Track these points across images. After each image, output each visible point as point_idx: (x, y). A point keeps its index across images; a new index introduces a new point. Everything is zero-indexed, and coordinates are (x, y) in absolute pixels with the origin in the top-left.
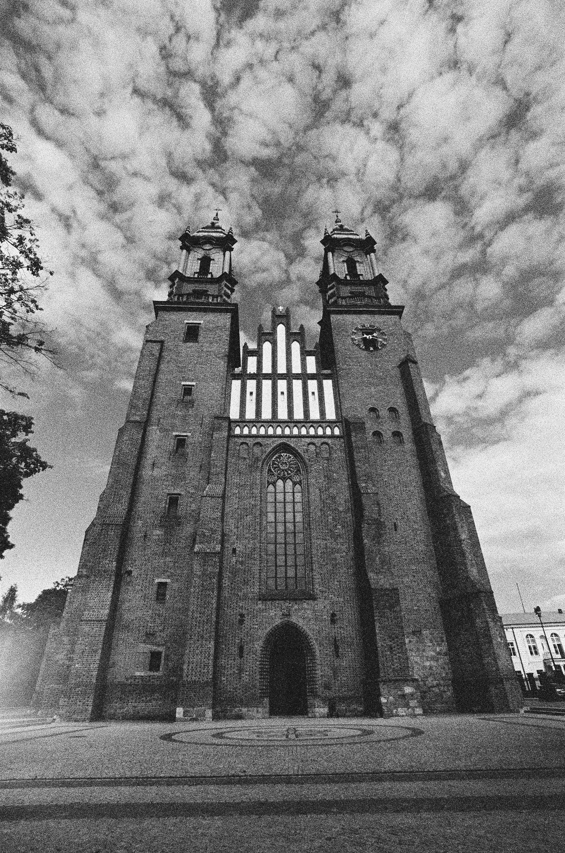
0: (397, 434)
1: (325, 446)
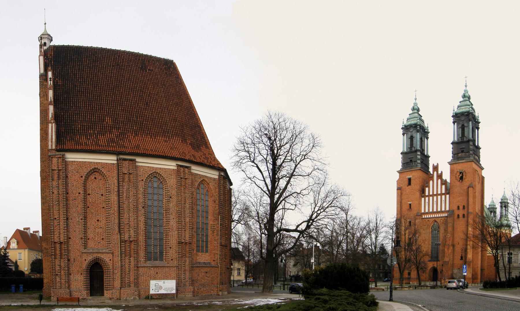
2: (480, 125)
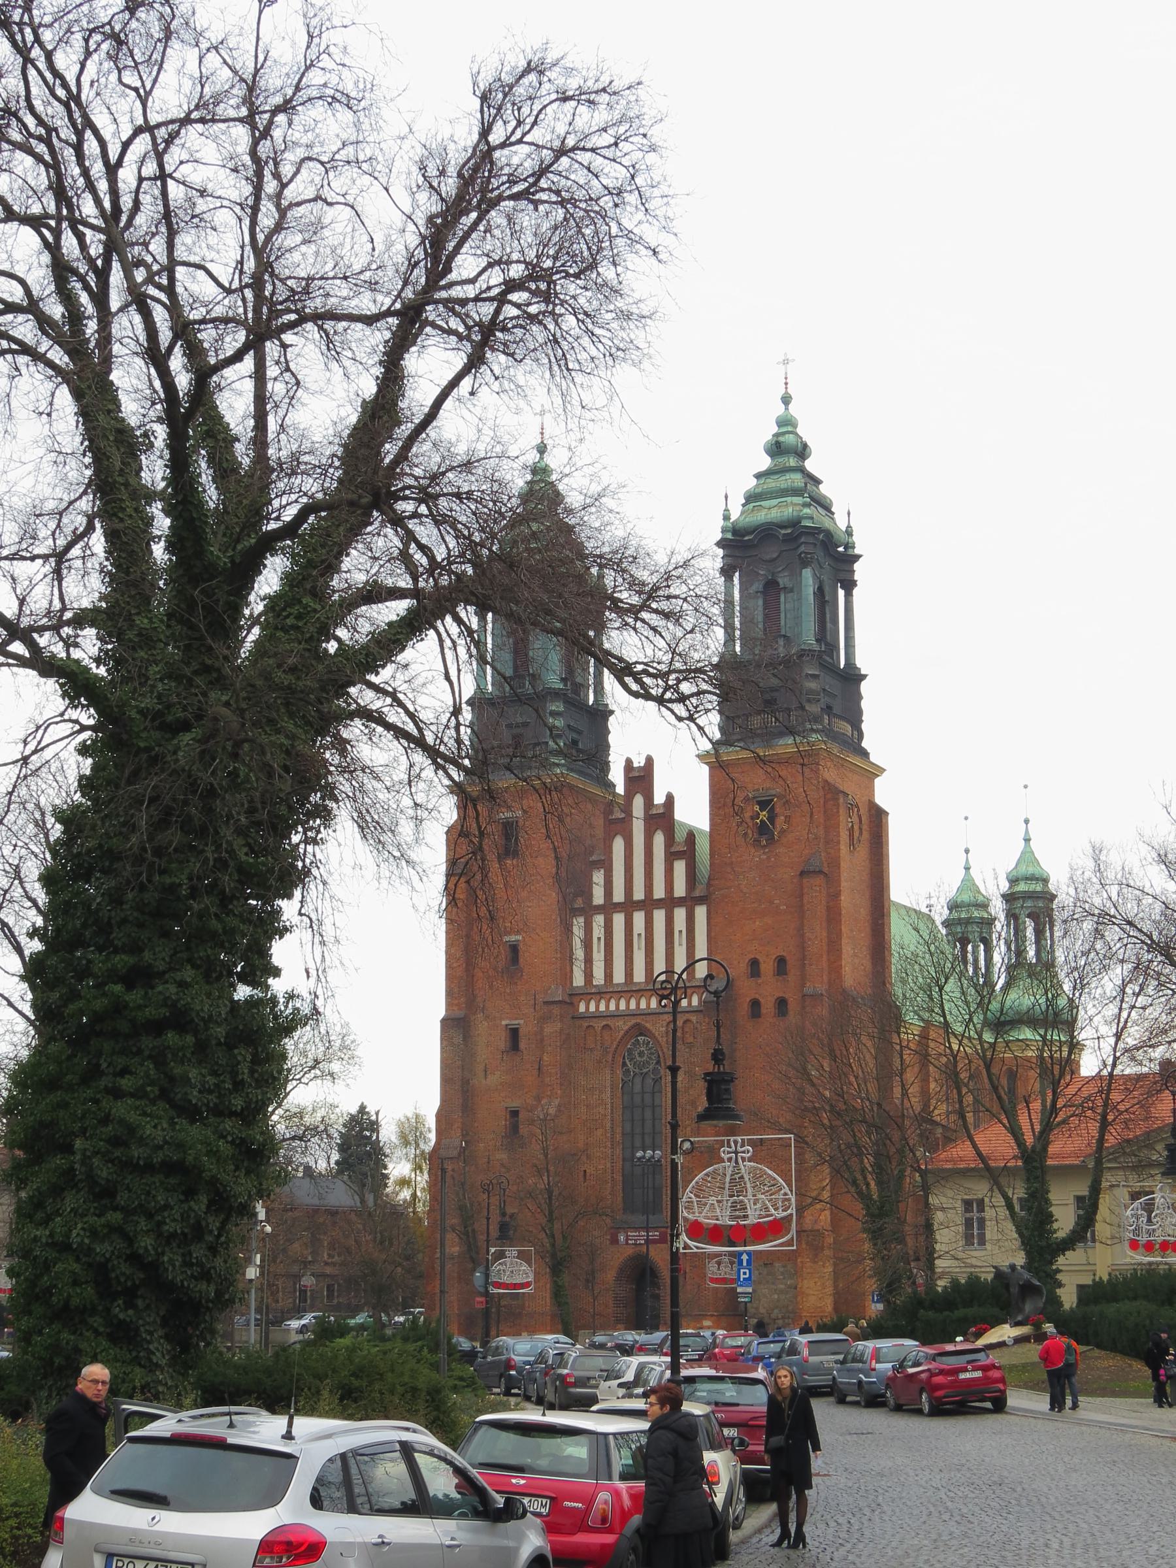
1: (688, 1024)
2: (860, 570)
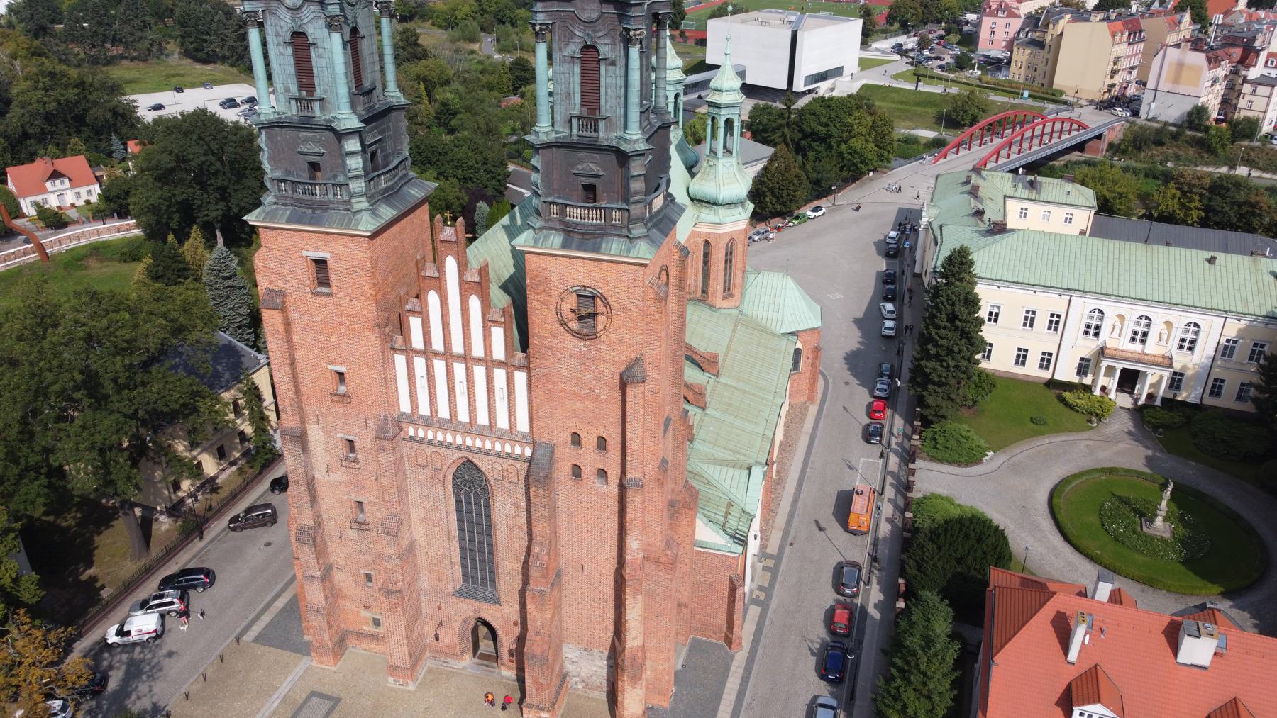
0: (602, 473)
